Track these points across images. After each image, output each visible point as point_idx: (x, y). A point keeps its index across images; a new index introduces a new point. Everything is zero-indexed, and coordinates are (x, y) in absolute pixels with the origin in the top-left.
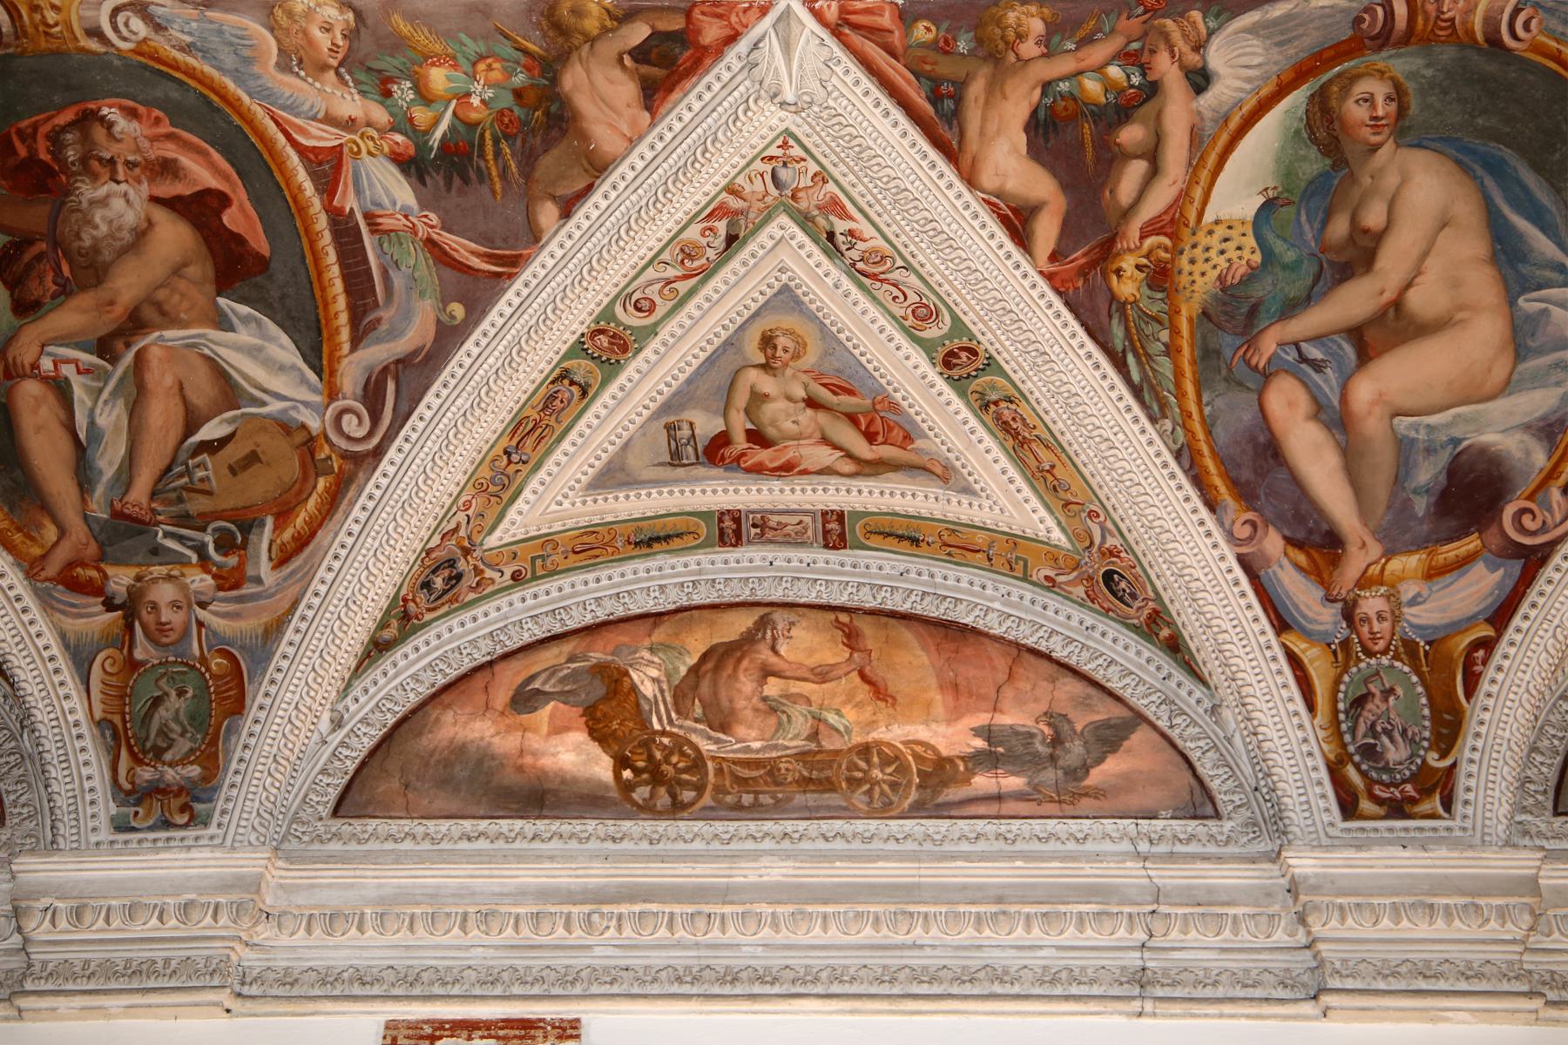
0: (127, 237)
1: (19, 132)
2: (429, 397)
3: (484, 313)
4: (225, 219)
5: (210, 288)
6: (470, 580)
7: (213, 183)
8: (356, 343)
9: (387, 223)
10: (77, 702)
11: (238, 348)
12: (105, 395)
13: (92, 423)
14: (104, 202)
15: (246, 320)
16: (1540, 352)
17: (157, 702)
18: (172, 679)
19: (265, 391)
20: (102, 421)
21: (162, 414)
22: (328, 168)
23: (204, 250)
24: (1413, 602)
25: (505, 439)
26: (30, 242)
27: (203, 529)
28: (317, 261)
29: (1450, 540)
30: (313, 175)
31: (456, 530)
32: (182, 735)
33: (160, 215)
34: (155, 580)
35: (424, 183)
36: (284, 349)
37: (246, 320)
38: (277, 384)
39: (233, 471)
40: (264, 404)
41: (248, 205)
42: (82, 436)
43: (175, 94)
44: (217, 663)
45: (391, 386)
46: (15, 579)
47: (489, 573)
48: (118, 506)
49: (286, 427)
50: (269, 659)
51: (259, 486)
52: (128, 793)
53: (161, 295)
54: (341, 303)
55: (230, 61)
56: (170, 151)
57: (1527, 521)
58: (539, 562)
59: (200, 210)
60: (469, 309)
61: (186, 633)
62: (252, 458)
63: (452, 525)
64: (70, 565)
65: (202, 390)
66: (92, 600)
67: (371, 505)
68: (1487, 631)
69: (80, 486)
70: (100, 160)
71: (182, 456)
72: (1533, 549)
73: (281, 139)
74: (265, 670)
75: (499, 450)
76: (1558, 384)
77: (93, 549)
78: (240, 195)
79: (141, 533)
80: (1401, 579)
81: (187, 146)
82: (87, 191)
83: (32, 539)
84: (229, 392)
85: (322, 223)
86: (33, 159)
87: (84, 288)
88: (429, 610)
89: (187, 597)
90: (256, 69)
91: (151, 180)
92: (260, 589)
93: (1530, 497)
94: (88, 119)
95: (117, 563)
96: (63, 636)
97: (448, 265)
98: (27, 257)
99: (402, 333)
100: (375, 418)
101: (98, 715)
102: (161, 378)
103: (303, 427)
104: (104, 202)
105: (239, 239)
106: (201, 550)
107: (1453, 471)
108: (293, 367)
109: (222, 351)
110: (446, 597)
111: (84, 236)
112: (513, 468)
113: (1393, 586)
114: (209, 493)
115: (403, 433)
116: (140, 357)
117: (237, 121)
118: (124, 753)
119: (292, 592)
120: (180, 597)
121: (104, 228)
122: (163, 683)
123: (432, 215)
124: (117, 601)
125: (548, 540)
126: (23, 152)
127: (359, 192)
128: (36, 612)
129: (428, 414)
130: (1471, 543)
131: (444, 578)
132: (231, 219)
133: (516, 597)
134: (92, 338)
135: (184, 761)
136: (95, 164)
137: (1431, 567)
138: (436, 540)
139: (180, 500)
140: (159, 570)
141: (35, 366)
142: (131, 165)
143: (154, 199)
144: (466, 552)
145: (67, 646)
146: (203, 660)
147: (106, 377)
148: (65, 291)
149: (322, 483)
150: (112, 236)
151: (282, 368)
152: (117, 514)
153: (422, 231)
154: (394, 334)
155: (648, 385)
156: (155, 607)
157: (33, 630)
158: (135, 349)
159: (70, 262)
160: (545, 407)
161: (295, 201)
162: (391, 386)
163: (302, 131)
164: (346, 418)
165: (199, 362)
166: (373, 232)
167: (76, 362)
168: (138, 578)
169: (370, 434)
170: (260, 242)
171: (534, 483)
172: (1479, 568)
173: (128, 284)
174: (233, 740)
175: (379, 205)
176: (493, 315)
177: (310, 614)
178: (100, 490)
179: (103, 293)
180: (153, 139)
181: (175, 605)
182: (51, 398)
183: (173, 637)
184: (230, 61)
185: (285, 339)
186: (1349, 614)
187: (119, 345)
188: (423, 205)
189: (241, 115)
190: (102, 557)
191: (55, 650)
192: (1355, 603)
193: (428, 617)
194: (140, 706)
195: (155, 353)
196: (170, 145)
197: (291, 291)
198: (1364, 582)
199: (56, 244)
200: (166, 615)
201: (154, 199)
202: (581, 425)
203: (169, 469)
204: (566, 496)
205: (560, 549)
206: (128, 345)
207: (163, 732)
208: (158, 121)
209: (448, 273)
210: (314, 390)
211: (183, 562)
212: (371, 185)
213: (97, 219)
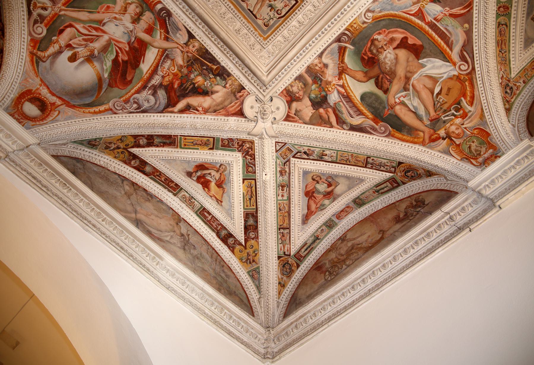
0: (394, 61)
1: (364, 54)
2: (475, 48)
3: (472, 21)
4: (409, 42)
5: (416, 60)
6: (515, 88)
7: (401, 36)
8: (451, 50)
9: (439, 17)
10: (453, 160)
11: (430, 69)
12: (412, 99)
13: (414, 106)
14: (386, 57)
15: (427, 62)
17: (470, 147)
18: (469, 141)
19: (441, 74)
20: (415, 104)
21: (425, 94)
22: (420, 14)
23: (409, 52)
25: (497, 48)
26: (379, 76)
27: (450, 110)
28: (432, 37)
30: (419, 19)
31: (503, 76)
32: (481, 148)
33: (398, 51)
34: (449, 127)
35: (440, 2)
36: (438, 62)
37: (427, 62)
38: (442, 71)
39: (447, 95)
40: (443, 77)
41: (411, 35)
42: (413, 110)
43: (383, 23)
44: (475, 132)
45: (465, 53)
46: (421, 148)
47: (518, 84)
48: (430, 119)
49: (451, 78)
50: (486, 122)
51: (455, 94)
52: (480, 165)
53: (408, 69)
54: (443, 43)
55: (389, 7)
56: (391, 36)
58: (526, 76)
59: (403, 44)
60: (469, 23)
61: (464, 132)
62: (449, 89)
63: (501, 76)
64: (430, 137)
65: (429, 83)
66: (439, 141)
67: (480, 79)
69: (420, 120)
70: (380, 48)
71: (435, 100)
73: (408, 16)
74: (488, 125)
75: (498, 52)
77: (432, 131)
78: (408, 35)
79: (439, 121)
81: (393, 32)
82: (382, 57)
83: (419, 138)
84: (434, 80)
85: (427, 28)
86: (369, 58)
87: (393, 79)
88: (512, 98)
89: (458, 125)
90: (395, 5)
91: (391, 45)
92: (472, 113)
94: (373, 41)
95: (439, 130)
96: (439, 151)
97: (457, 17)
98: (380, 80)
99: (459, 40)
100: (467, 62)
101: (460, 159)
102: (419, 87)
103: (454, 75)
104: (386, 57)
105: (414, 45)
106: (453, 115)
108: (443, 65)
109: (427, 72)
110: (513, 94)
111: (387, 67)
112: (504, 55)
114: (446, 102)
115: (475, 60)
116: (413, 85)
117: (398, 19)
118: (472, 160)
119: (479, 107)
120: (456, 127)
121: (389, 63)
122: (468, 143)
123: (447, 8)
124: (445, 137)
125: (524, 70)
126: (366, 58)
127: (429, 15)
128: (430, 151)
129: (477, 52)
131: (509, 90)
132: (410, 42)
133: (528, 87)
134: (402, 88)
135: (486, 151)
136: (380, 50)
138: (501, 81)
139: (441, 108)
140: (448, 125)
141: (395, 102)
142: (386, 45)
143: (394, 49)
144: (509, 81)
145: (442, 152)
146: (472, 133)
147: (409, 94)
148: (391, 82)
149: (467, 83)
150: (392, 63)
151: (441, 67)
152: (431, 121)
153: (447, 14)
154: (457, 41)
155: (518, 32)
156: (453, 132)
157: (432, 154)
158: (411, 85)
159: (388, 75)
160: (501, 35)
161: (419, 27)
162: (465, 53)
163: (411, 11)
164: (461, 67)
165: (424, 78)
166: (438, 22)
167: (402, 96)
168: (445, 130)
169: (469, 66)
170: (419, 42)
171: (511, 56)
173: (401, 72)
174: (493, 140)
175: (435, 15)
176: (475, 19)
177: (487, 107)
178: (424, 118)
179: (398, 77)
180: (386, 36)
181: (457, 129)
182: (403, 107)
183: (462, 134)
184: (389, 7)
185: (437, 60)
187: (407, 86)
188: (443, 7)
189: (398, 17)
190: (435, 131)
191: (440, 154)
193: (513, 100)
194: (467, 150)
195: (415, 82)
196: (390, 34)
197: (431, 48)
199: (383, 73)
200: (457, 132)
201: (394, 49)
202: (512, 34)
203: (434, 104)
204: (521, 53)
205: (529, 70)
206: (409, 85)
207: (476, 151)
208: (385, 31)
209: (459, 19)
210: (451, 66)
211: (451, 120)
212: (431, 11)
213: (387, 62)
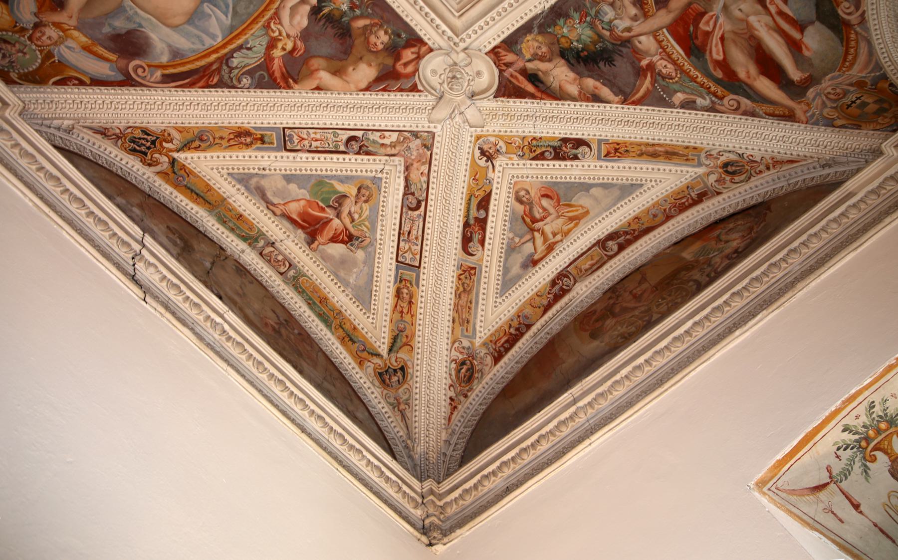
16: (197, 27)
24: (69, 48)
29: (106, 48)
57: (140, 71)
68: (88, 82)
72: (133, 80)
76: (193, 43)
80: (72, 38)
93: (149, 66)
107: (129, 32)
113: (67, 37)
130: (113, 57)
137: (88, 47)
172: (107, 65)
186: (36, 26)
192: (45, 26)
198: (57, 25)
